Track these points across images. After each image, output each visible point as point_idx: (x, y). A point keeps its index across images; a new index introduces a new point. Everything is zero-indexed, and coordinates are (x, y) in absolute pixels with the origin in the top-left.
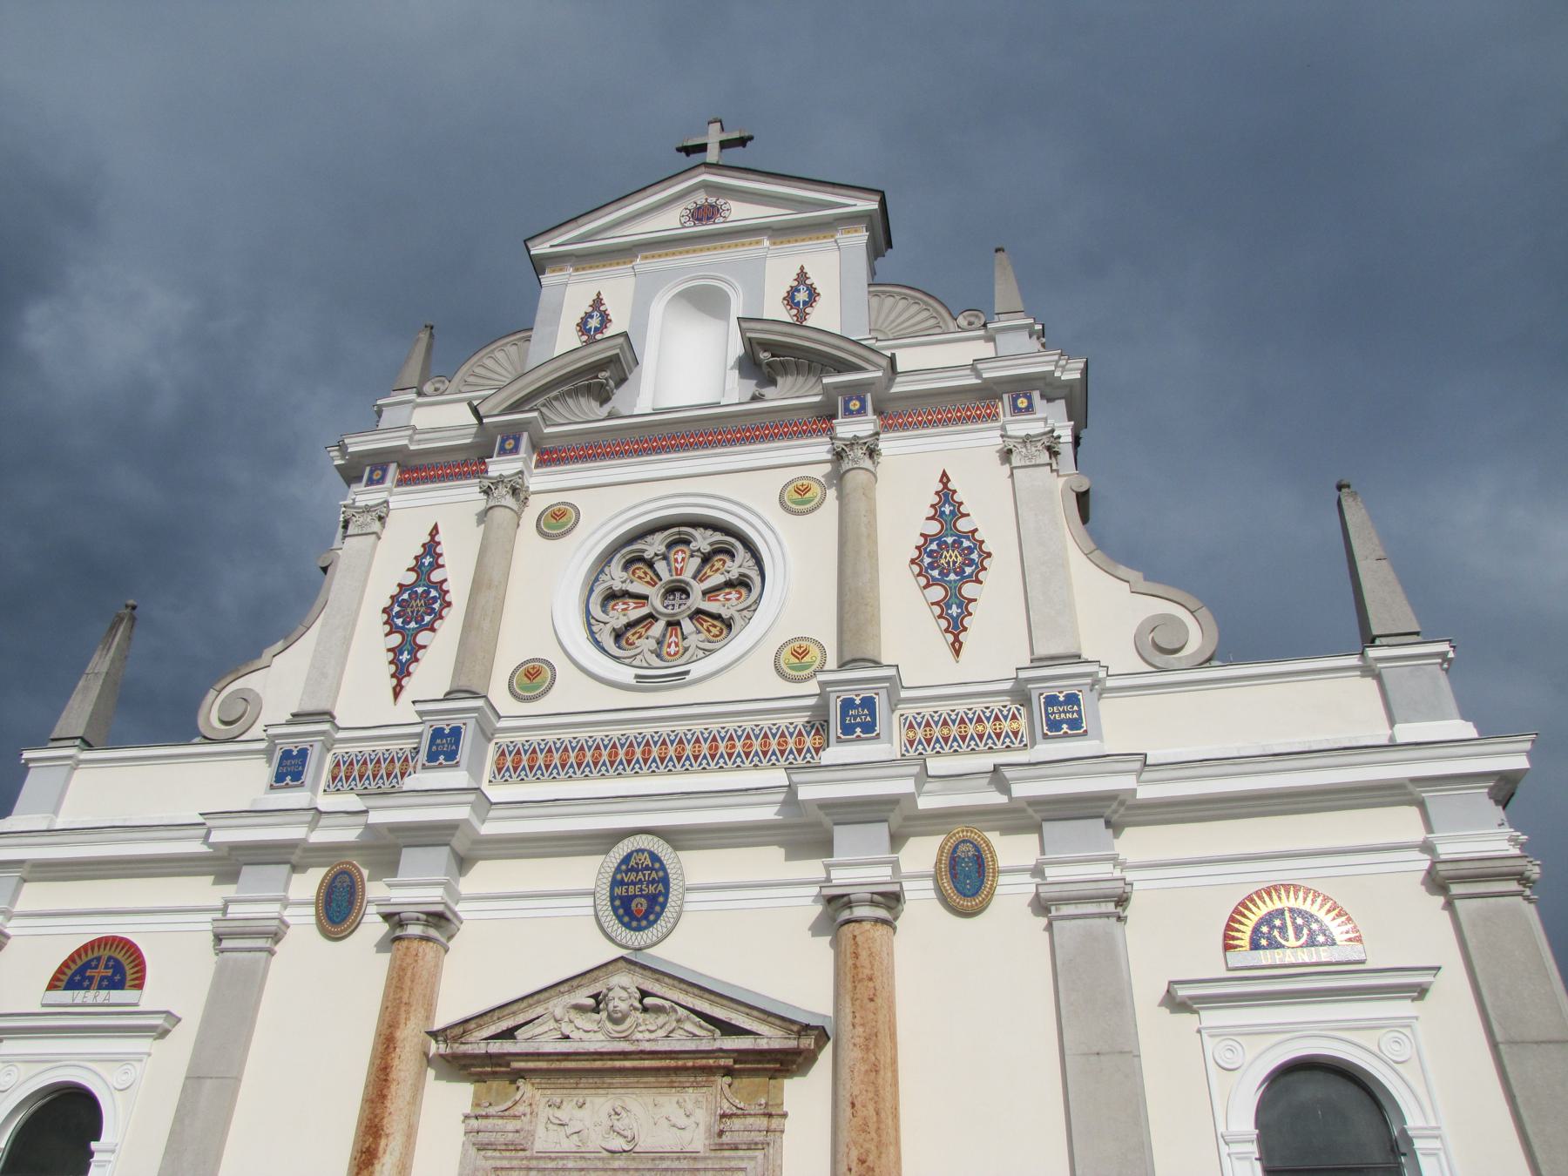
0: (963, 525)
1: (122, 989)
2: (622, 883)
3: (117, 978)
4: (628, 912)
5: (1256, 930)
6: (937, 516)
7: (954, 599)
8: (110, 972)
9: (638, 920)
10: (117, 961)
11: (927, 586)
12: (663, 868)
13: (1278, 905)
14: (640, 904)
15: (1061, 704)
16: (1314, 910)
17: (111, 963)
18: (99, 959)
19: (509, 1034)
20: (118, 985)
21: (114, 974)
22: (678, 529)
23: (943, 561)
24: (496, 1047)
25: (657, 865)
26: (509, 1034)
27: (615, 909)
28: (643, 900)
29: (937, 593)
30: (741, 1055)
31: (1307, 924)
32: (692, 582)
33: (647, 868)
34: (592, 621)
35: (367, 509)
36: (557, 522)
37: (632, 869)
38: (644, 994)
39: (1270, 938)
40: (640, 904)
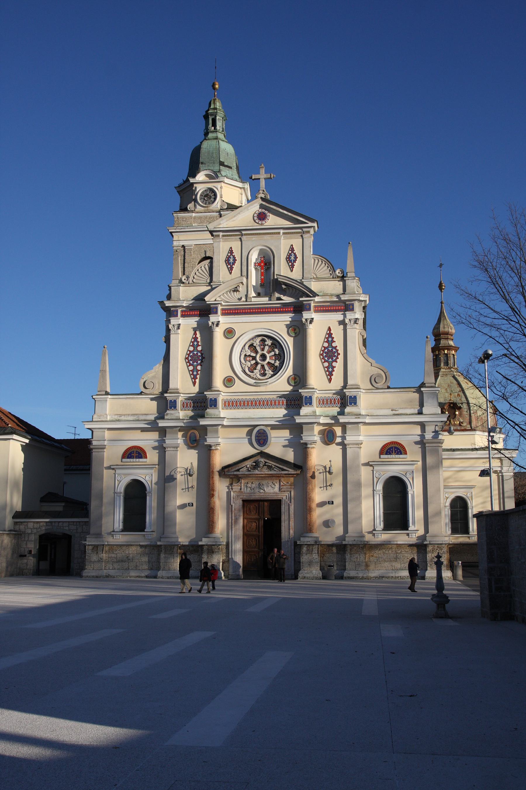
0: (334, 345)
1: (142, 458)
3: (140, 456)
7: (330, 366)
8: (137, 455)
9: (262, 444)
10: (138, 452)
11: (324, 362)
13: (392, 446)
16: (399, 447)
17: (137, 452)
18: (134, 451)
19: (238, 470)
21: (139, 455)
23: (328, 355)
24: (236, 473)
25: (265, 433)
26: (238, 470)
28: (262, 440)
29: (326, 364)
30: (286, 474)
31: (397, 450)
32: (267, 354)
33: (263, 433)
34: (242, 364)
37: (259, 433)
38: (266, 462)
40: (262, 441)
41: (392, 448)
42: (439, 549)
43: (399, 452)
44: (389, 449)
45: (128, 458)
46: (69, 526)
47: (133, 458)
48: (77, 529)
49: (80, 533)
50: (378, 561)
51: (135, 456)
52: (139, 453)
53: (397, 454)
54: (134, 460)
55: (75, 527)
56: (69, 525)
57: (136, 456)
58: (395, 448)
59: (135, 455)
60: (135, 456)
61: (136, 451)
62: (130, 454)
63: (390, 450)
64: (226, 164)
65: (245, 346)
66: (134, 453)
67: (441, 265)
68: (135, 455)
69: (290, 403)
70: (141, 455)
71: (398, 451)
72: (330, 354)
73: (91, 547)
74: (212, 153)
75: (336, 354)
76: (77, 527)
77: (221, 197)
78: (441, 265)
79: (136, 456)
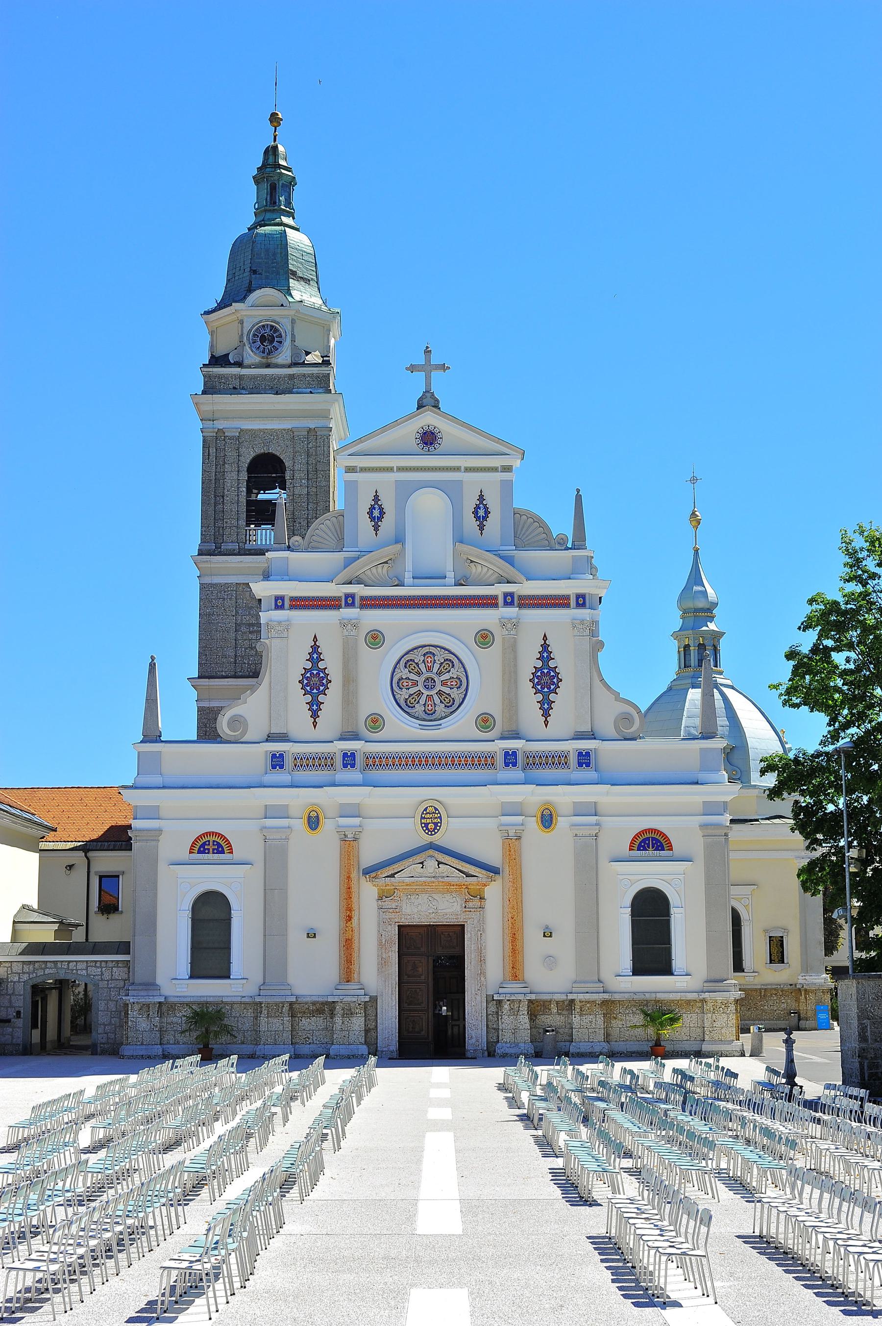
2: (424, 818)
3: (220, 849)
4: (427, 829)
5: (641, 842)
6: (541, 658)
7: (546, 701)
10: (217, 842)
12: (439, 813)
14: (431, 826)
15: (583, 756)
18: (209, 841)
19: (392, 876)
20: (223, 852)
21: (218, 848)
22: (429, 651)
23: (542, 682)
25: (437, 812)
26: (392, 876)
27: (422, 827)
28: (432, 824)
33: (433, 813)
35: (280, 622)
36: (375, 639)
39: (643, 847)
40: (431, 826)
41: (648, 839)
42: (723, 1006)
43: (659, 846)
44: (644, 841)
45: (199, 852)
46: (87, 969)
47: (208, 853)
48: (102, 974)
49: (108, 981)
50: (624, 1026)
51: (211, 850)
52: (219, 845)
53: (657, 849)
54: (210, 856)
55: (99, 970)
56: (87, 967)
57: (214, 849)
58: (653, 839)
59: (211, 847)
60: (211, 850)
61: (214, 841)
62: (204, 844)
63: (645, 843)
64: (300, 274)
65: (398, 662)
66: (209, 845)
67: (694, 480)
68: (211, 847)
69: (478, 761)
70: (222, 847)
71: (657, 845)
72: (546, 679)
73: (136, 1007)
74: (274, 254)
75: (555, 680)
76: (101, 971)
77: (293, 340)
78: (694, 480)
79: (214, 849)
